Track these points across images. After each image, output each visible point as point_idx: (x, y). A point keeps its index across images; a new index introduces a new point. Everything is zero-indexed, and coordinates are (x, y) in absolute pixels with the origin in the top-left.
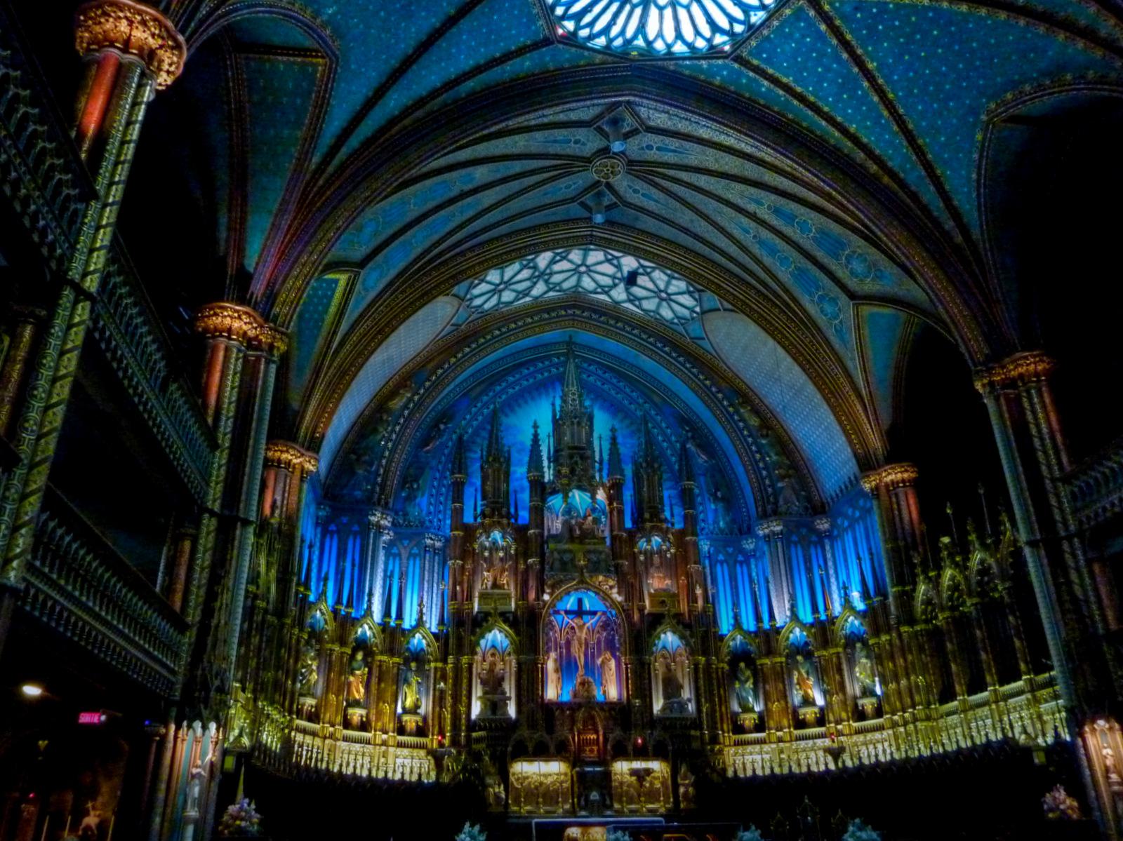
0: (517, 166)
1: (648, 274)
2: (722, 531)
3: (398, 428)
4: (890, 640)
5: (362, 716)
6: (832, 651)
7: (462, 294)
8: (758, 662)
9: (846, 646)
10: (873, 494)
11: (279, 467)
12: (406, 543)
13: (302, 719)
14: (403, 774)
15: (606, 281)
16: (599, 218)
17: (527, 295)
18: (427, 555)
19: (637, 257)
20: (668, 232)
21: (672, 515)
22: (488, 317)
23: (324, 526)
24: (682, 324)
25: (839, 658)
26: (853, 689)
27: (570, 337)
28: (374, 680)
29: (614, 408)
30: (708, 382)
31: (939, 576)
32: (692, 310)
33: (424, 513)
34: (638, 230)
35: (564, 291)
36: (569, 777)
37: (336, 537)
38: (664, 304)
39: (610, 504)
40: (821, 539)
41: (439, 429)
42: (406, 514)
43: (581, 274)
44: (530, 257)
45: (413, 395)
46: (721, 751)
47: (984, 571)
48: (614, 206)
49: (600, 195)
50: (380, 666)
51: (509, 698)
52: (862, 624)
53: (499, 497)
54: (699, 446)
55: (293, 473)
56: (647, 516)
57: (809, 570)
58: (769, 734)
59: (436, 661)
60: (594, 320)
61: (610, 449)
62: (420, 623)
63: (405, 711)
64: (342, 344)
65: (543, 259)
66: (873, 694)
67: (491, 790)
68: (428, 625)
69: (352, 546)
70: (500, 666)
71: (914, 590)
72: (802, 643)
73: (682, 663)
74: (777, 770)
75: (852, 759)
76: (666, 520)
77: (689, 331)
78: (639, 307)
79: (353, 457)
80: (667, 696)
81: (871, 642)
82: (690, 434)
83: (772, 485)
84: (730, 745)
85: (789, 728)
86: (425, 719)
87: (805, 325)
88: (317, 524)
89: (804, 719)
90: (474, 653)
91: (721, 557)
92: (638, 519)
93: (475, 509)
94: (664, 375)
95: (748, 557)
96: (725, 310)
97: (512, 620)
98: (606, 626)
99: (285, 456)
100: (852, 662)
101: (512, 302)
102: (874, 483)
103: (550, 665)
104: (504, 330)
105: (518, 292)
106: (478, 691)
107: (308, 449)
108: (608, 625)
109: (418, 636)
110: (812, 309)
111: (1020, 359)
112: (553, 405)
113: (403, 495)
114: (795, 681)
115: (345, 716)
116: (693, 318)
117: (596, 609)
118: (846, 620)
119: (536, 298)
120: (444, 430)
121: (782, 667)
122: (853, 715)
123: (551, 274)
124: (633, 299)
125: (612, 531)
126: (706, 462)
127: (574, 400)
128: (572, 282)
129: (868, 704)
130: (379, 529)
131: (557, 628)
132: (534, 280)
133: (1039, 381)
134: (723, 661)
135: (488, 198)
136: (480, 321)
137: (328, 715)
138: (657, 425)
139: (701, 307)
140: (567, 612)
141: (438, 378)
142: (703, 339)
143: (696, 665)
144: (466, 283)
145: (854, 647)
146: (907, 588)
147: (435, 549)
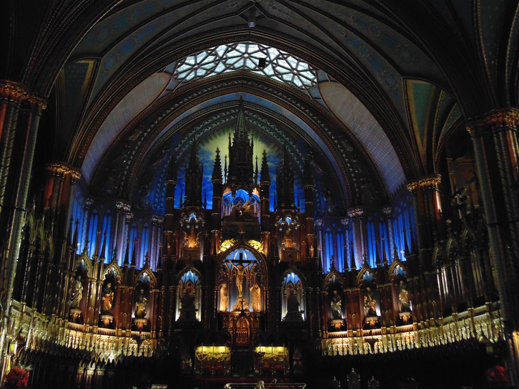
1: (285, 59)
2: (329, 214)
3: (134, 153)
4: (419, 279)
5: (110, 320)
6: (387, 285)
8: (345, 291)
9: (394, 282)
10: (413, 194)
11: (56, 176)
12: (141, 220)
13: (72, 322)
14: (133, 353)
16: (252, 25)
17: (213, 72)
18: (154, 228)
19: (278, 48)
20: (296, 33)
21: (299, 205)
22: (190, 85)
23: (90, 211)
24: (307, 90)
25: (390, 289)
26: (397, 307)
27: (241, 97)
28: (118, 299)
29: (266, 140)
31: (446, 243)
32: (312, 81)
33: (152, 203)
34: (278, 31)
35: (236, 69)
36: (230, 355)
37: (96, 217)
38: (296, 77)
39: (260, 198)
40: (385, 220)
41: (162, 152)
43: (245, 58)
44: (212, 48)
45: (143, 133)
46: (320, 341)
47: (469, 240)
49: (253, 10)
50: (122, 291)
51: (197, 310)
52: (404, 270)
55: (65, 179)
56: (283, 205)
57: (378, 238)
58: (348, 332)
59: (155, 288)
60: (255, 87)
61: (262, 165)
62: (146, 266)
63: (137, 317)
64: (94, 102)
65: (221, 50)
66: (408, 310)
67: (184, 362)
68: (151, 268)
69: (106, 222)
70: (193, 291)
71: (433, 250)
72: (371, 280)
73: (300, 290)
74: (351, 353)
75: (393, 348)
76: (295, 208)
77: (312, 94)
78: (281, 79)
79: (107, 169)
81: (408, 280)
82: (313, 156)
83: (359, 187)
84: (326, 338)
85: (360, 329)
86: (149, 321)
87: (377, 91)
88: (85, 209)
89: (369, 324)
90: (177, 284)
91: (328, 229)
92: (278, 207)
93: (181, 201)
94: (297, 120)
95: (343, 230)
96: (331, 81)
98: (256, 269)
99: (59, 170)
100: (398, 293)
101: (204, 76)
102: (414, 187)
103: (222, 291)
105: (207, 70)
106: (179, 306)
107: (74, 165)
108: (258, 269)
109: (145, 274)
110: (381, 82)
111: (493, 113)
112: (230, 138)
113: (140, 192)
114: (365, 302)
115: (100, 319)
116: (313, 86)
117: (249, 259)
118: (395, 267)
119: (219, 73)
121: (358, 294)
122: (397, 322)
123: (227, 59)
124: (277, 74)
125: (261, 214)
126: (322, 173)
127: (241, 135)
129: (405, 316)
130: (123, 212)
132: (216, 62)
134: (324, 290)
136: (184, 88)
137: (89, 320)
138: (293, 151)
139: (317, 80)
140: (233, 261)
142: (320, 98)
143: (307, 292)
144: (173, 64)
145: (399, 283)
146: (429, 249)
147: (159, 224)
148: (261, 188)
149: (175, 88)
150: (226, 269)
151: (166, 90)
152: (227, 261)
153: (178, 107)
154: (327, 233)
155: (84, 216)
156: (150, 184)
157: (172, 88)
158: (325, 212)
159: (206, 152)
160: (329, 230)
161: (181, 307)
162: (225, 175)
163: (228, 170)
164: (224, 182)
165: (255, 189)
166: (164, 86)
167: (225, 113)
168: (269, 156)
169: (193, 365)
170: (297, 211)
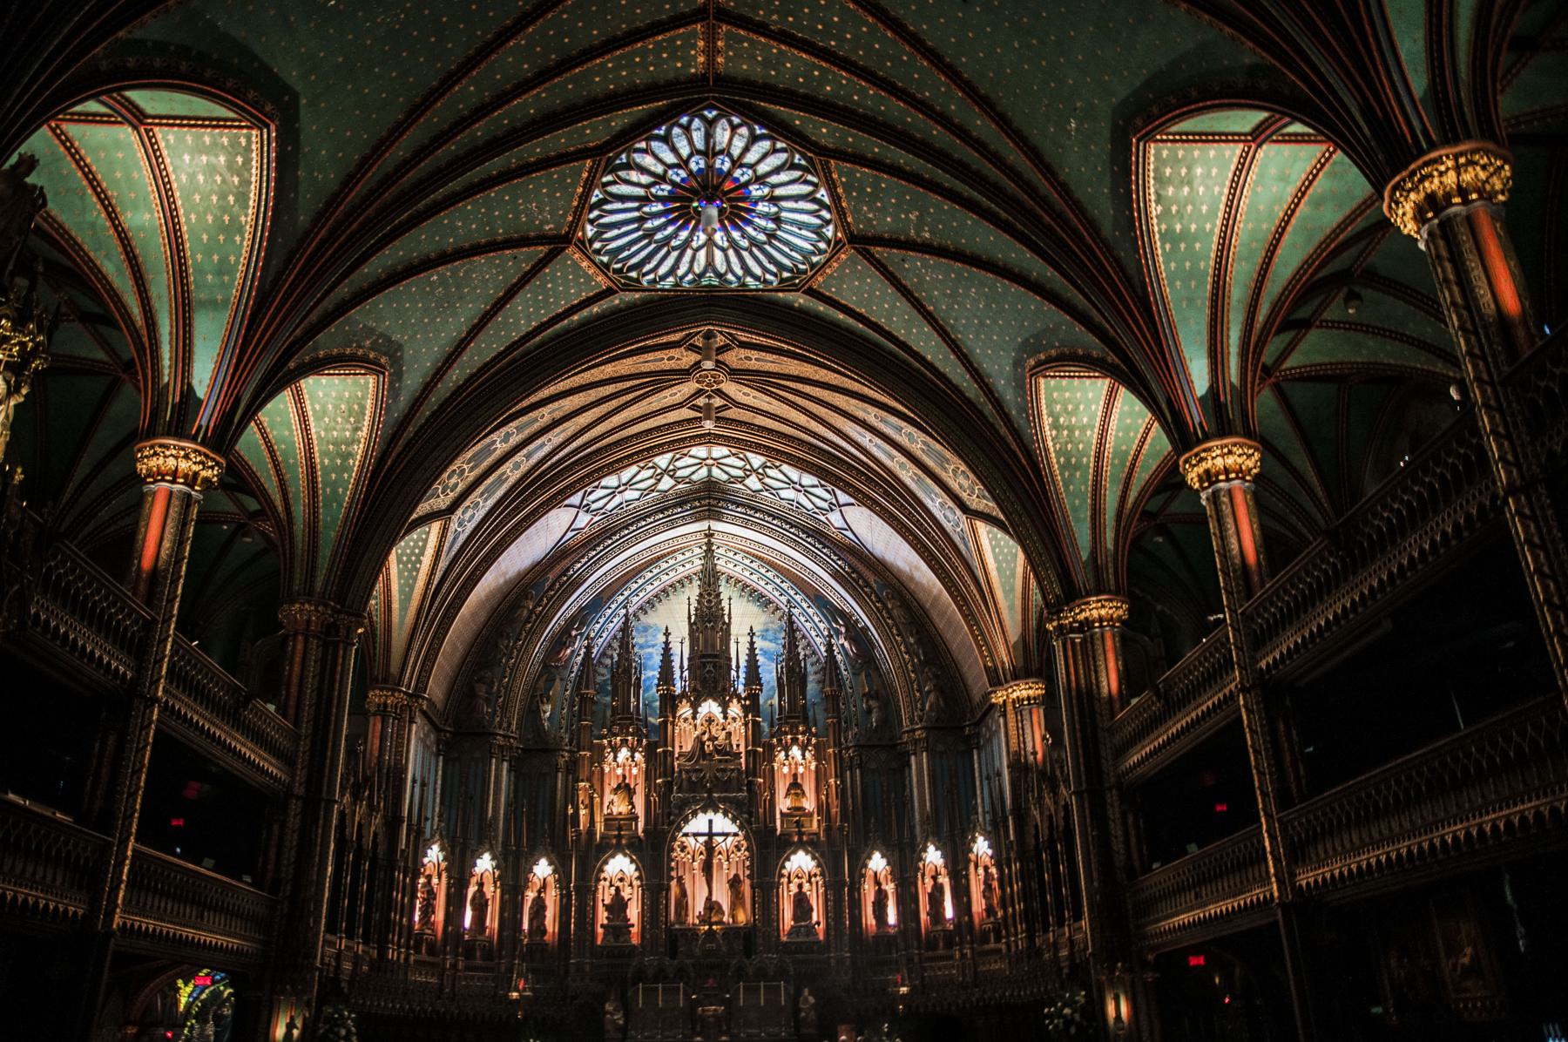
0: (611, 389)
7: (577, 503)
15: (740, 473)
39: (746, 716)
41: (570, 635)
45: (535, 607)
48: (724, 408)
65: (662, 461)
80: (795, 918)
97: (635, 848)
98: (738, 848)
117: (726, 831)
124: (768, 488)
125: (746, 747)
128: (703, 472)
131: (689, 849)
133: (1101, 626)
135: (583, 420)
140: (696, 835)
148: (745, 699)
150: (685, 847)
152: (686, 835)
155: (437, 765)
161: (605, 922)
162: (681, 677)
164: (678, 691)
165: (735, 701)
168: (767, 630)
169: (626, 1022)
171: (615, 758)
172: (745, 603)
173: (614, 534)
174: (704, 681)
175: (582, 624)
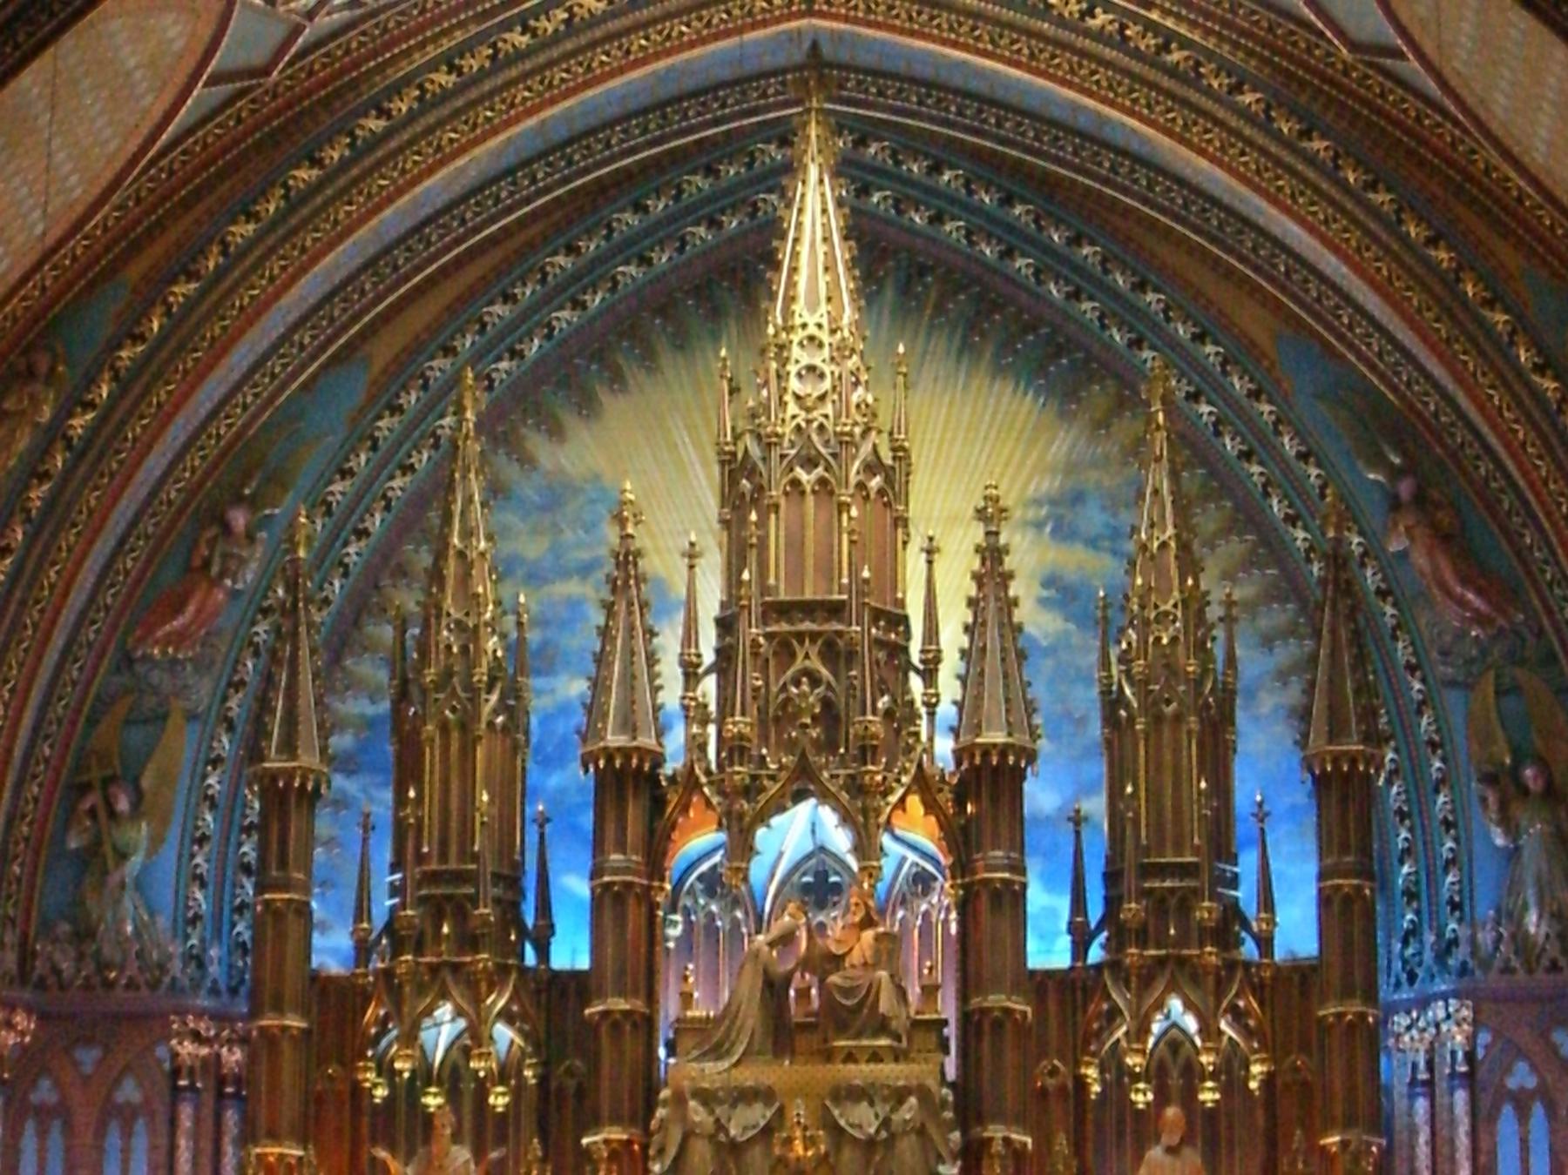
12: (88, 1057)
18: (186, 1114)
30: (1442, 255)
33: (163, 922)
39: (962, 867)
41: (227, 529)
42: (84, 934)
45: (64, 413)
53: (466, 854)
54: (1446, 539)
82: (1405, 488)
91: (1521, 1077)
93: (362, 910)
104: (472, 64)
113: (73, 844)
120: (250, 538)
125: (963, 996)
141: (175, 321)
142: (1400, 55)
147: (221, 1081)
149: (274, 62)
151: (206, 85)
153: (316, 188)
154: (1507, 1110)
156: (146, 783)
157: (258, 58)
158: (1499, 939)
159: (577, 491)
160: (1531, 1083)
163: (709, 657)
166: (190, 64)
167: (710, 171)
168: (1077, 498)
170: (1249, 950)
171: (410, 1037)
172: (980, 381)
173: (396, 90)
174: (775, 719)
175: (278, 481)
